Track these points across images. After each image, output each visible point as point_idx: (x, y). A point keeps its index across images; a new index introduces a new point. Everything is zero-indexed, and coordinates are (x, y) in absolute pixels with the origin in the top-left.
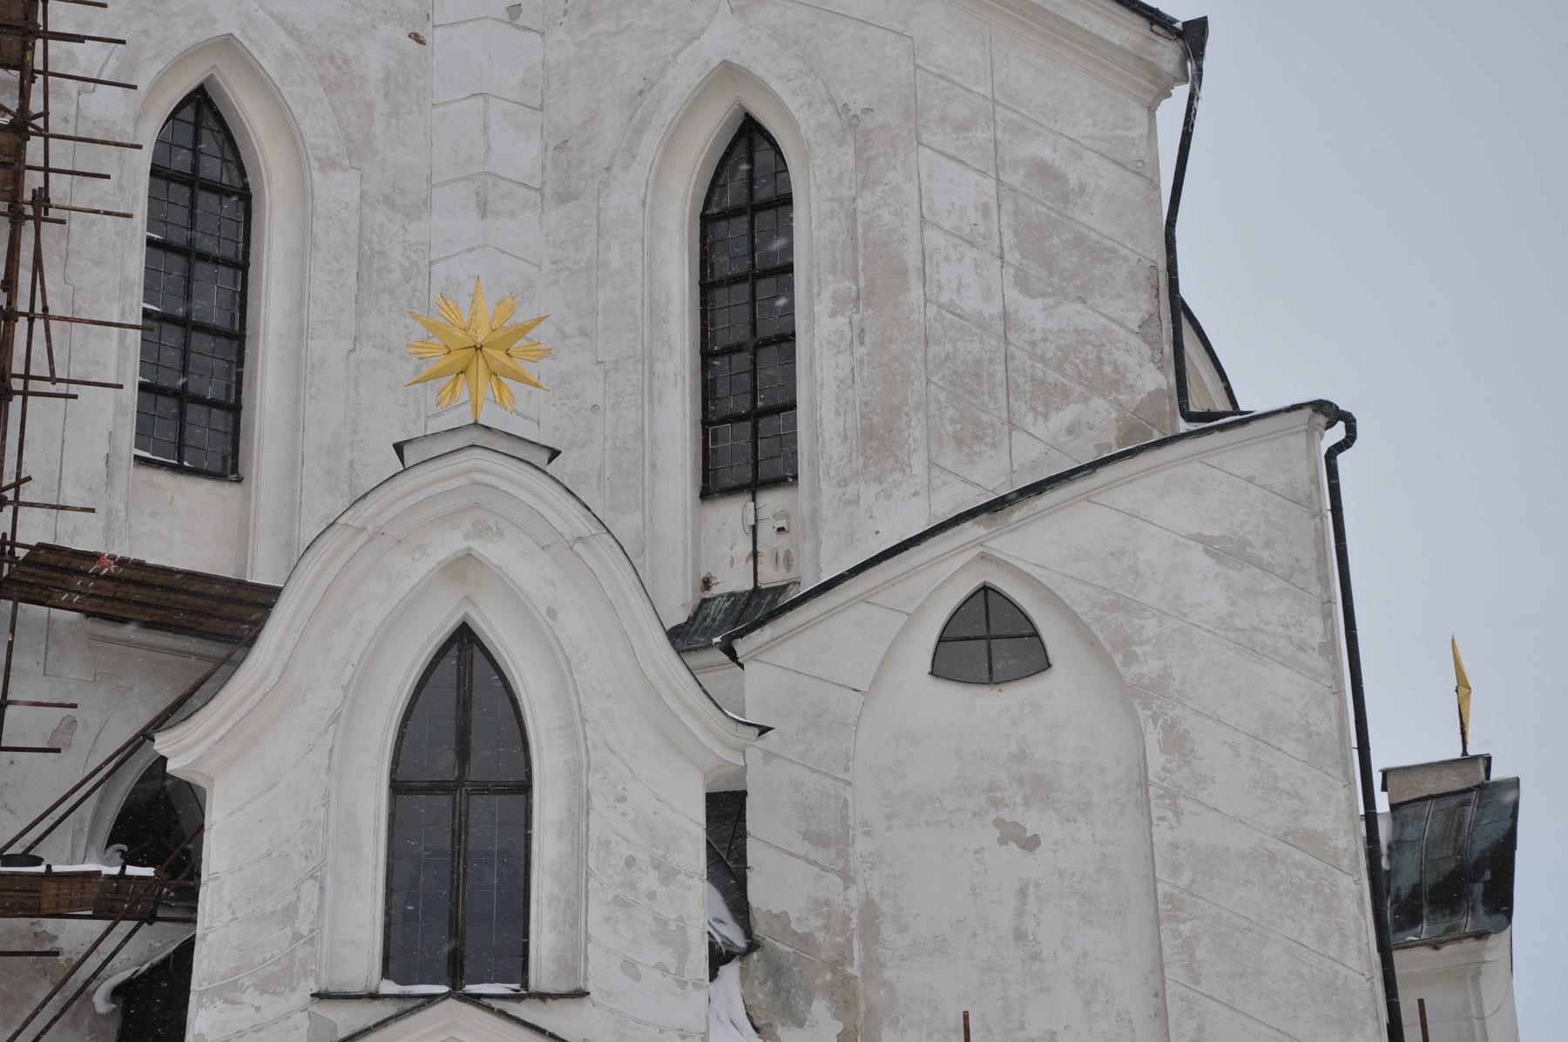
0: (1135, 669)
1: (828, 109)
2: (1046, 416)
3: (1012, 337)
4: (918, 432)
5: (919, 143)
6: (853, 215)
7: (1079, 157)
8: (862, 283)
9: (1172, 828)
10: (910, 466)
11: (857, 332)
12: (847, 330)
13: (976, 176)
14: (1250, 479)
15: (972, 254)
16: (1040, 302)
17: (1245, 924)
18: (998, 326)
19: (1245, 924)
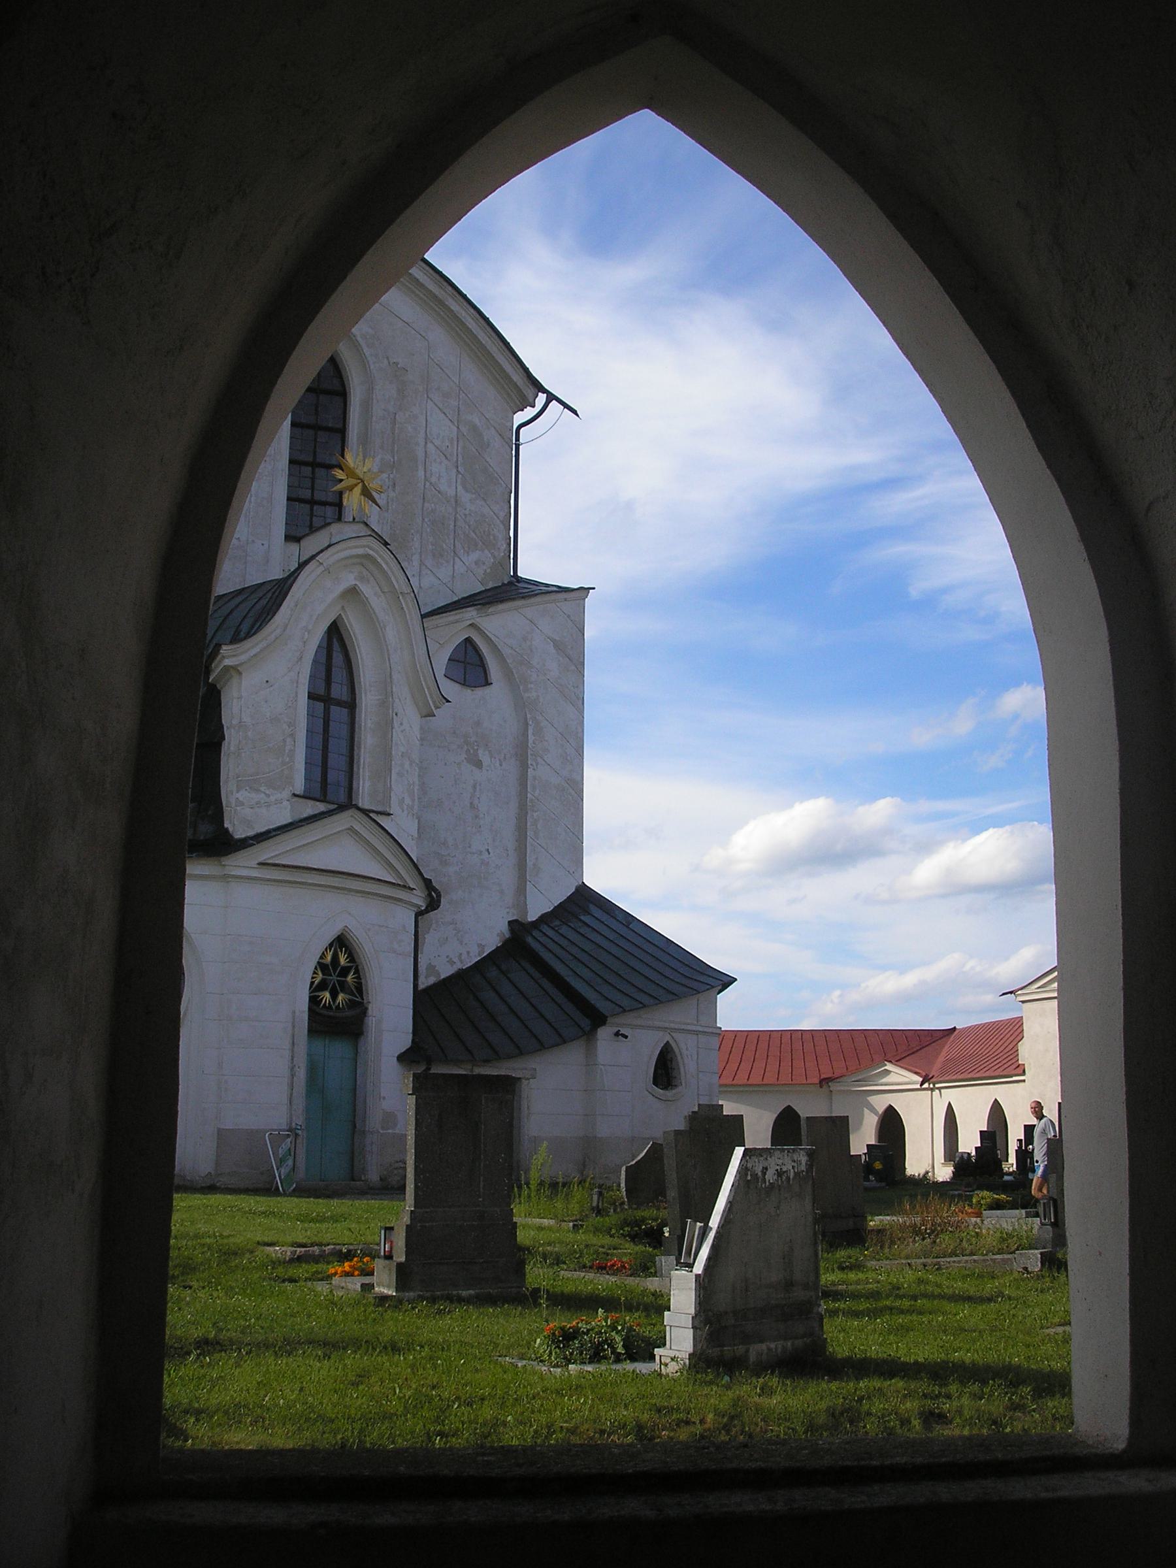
0: (526, 695)
1: (386, 361)
2: (468, 553)
3: (458, 509)
4: (417, 545)
5: (428, 397)
6: (394, 421)
7: (489, 428)
8: (396, 458)
9: (534, 769)
10: (411, 560)
11: (391, 483)
12: (387, 480)
13: (450, 424)
14: (569, 616)
15: (446, 462)
16: (469, 496)
17: (554, 817)
18: (453, 500)
19: (554, 817)
